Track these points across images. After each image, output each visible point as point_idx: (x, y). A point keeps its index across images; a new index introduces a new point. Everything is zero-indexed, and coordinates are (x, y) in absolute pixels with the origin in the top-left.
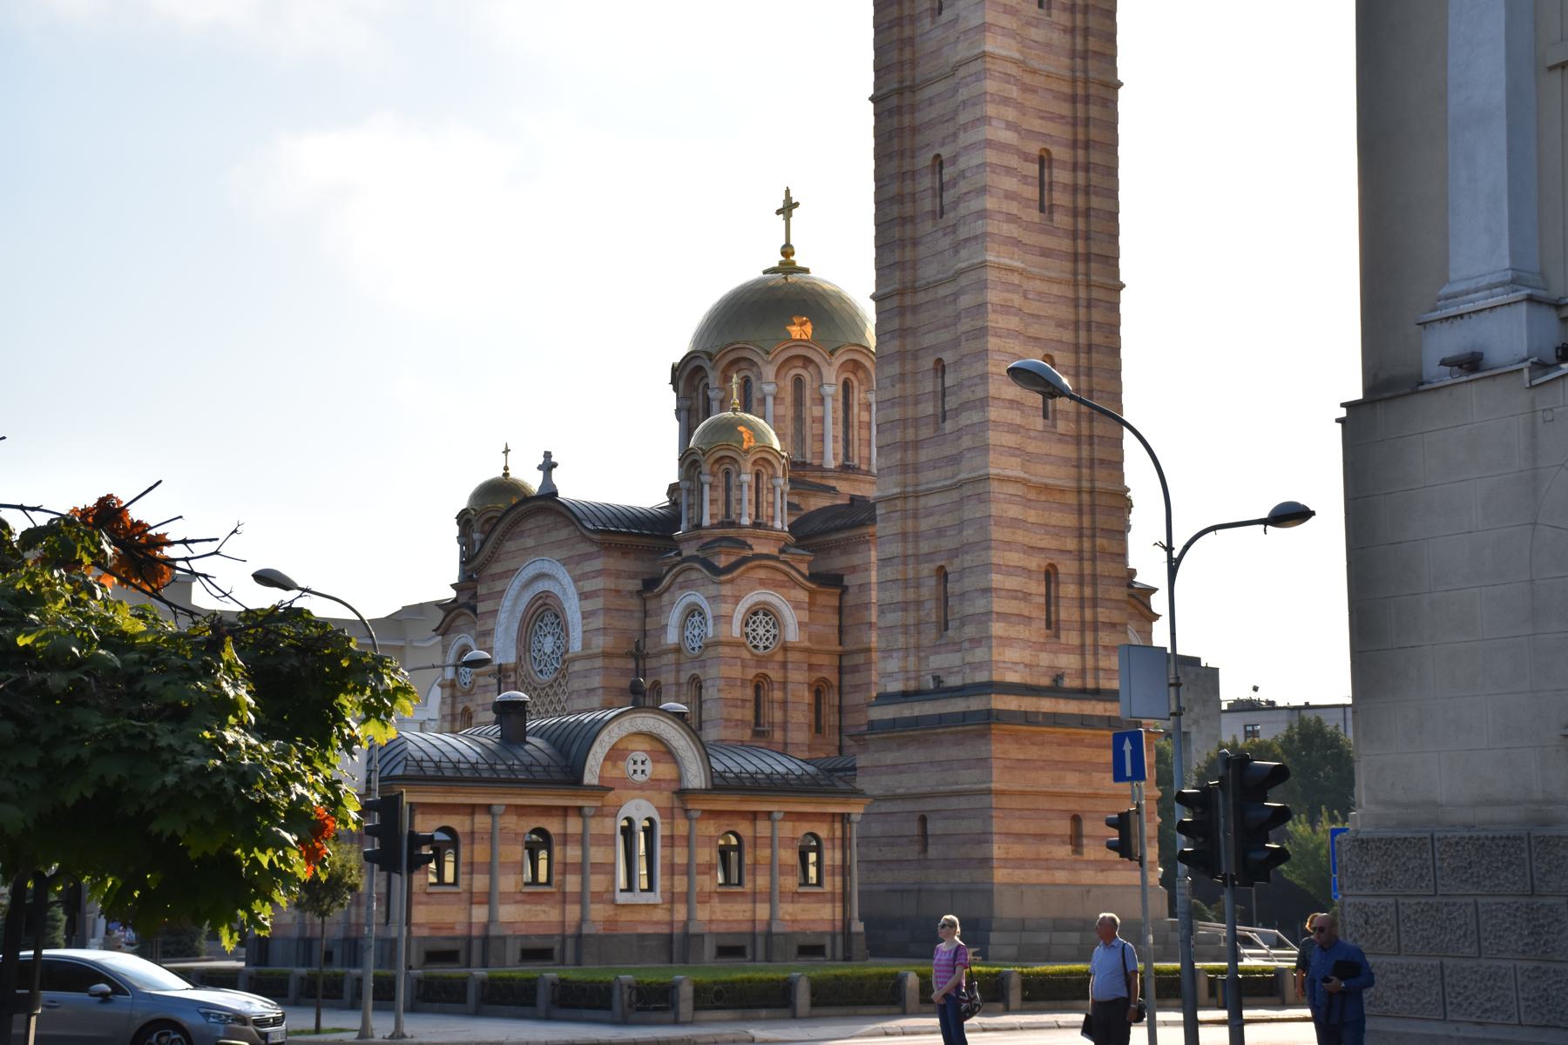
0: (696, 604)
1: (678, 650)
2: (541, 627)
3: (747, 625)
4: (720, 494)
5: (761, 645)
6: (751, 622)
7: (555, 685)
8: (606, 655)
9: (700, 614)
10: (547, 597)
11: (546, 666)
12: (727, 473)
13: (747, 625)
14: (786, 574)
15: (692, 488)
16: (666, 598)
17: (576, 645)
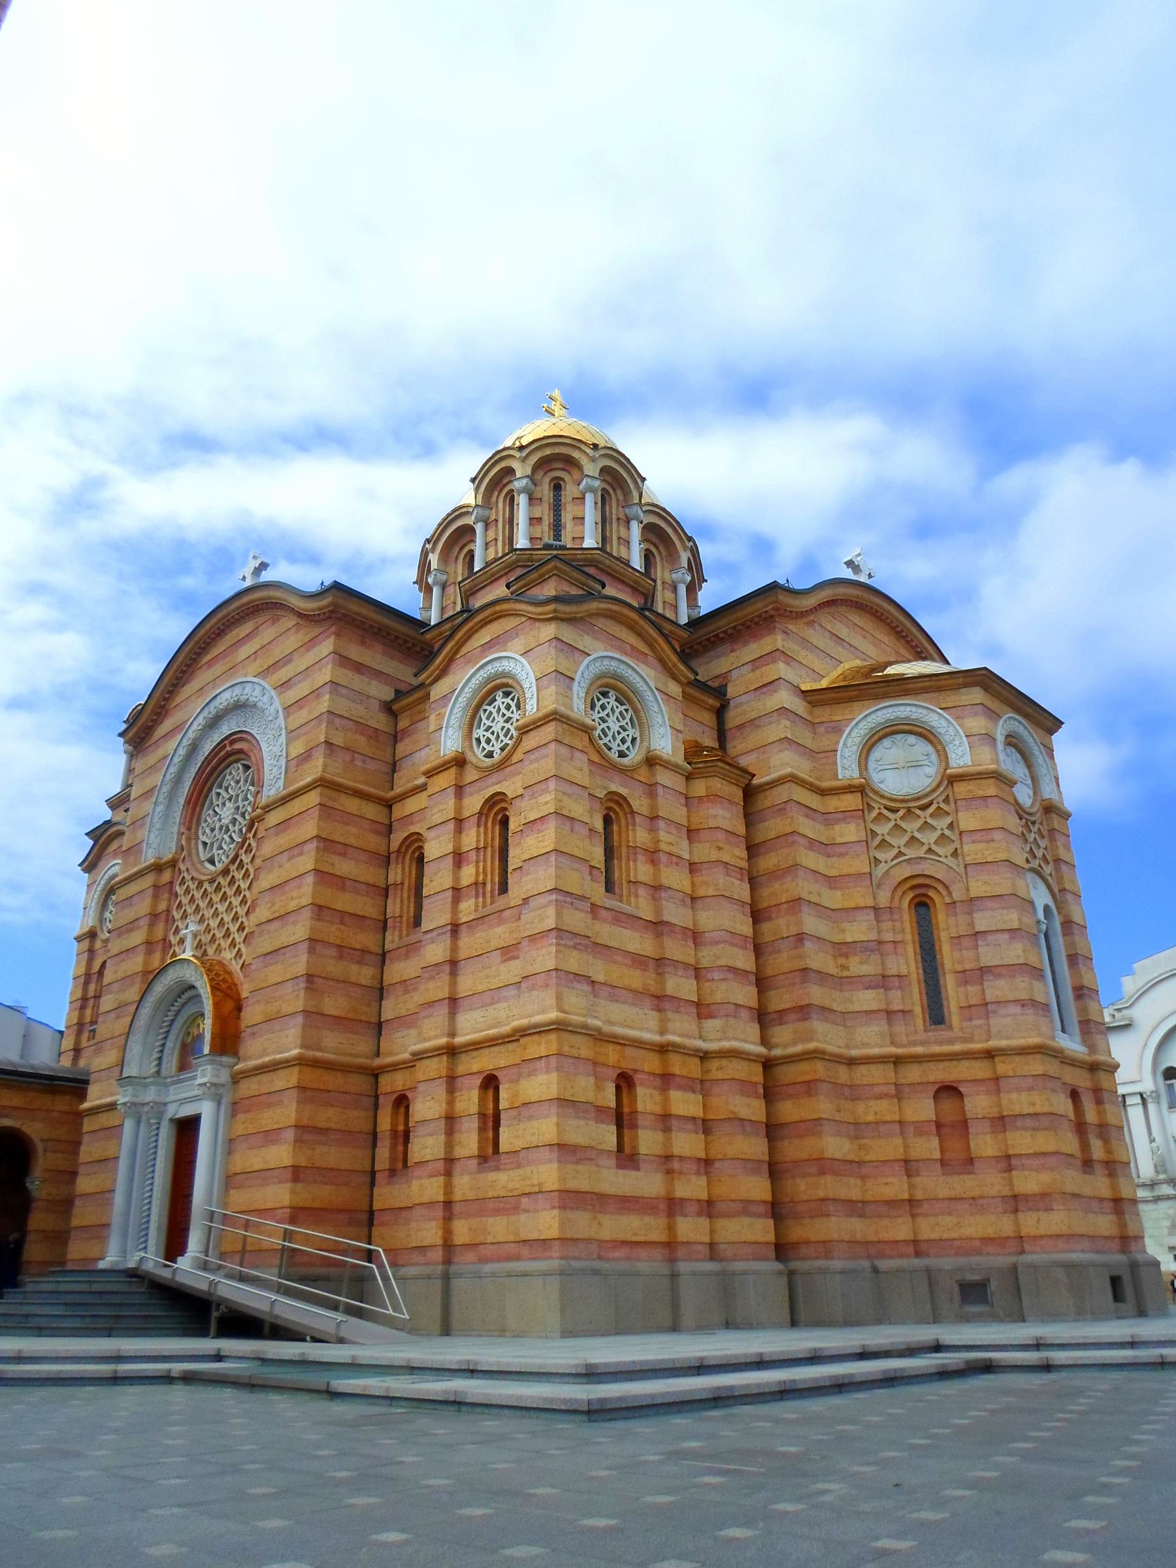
0: (504, 674)
1: (460, 762)
2: (218, 794)
3: (593, 707)
4: (544, 511)
5: (615, 747)
6: (598, 704)
7: (233, 868)
8: (322, 783)
9: (507, 694)
10: (232, 743)
11: (220, 848)
12: (557, 487)
13: (593, 707)
14: (651, 646)
15: (493, 517)
16: (437, 691)
17: (274, 784)
